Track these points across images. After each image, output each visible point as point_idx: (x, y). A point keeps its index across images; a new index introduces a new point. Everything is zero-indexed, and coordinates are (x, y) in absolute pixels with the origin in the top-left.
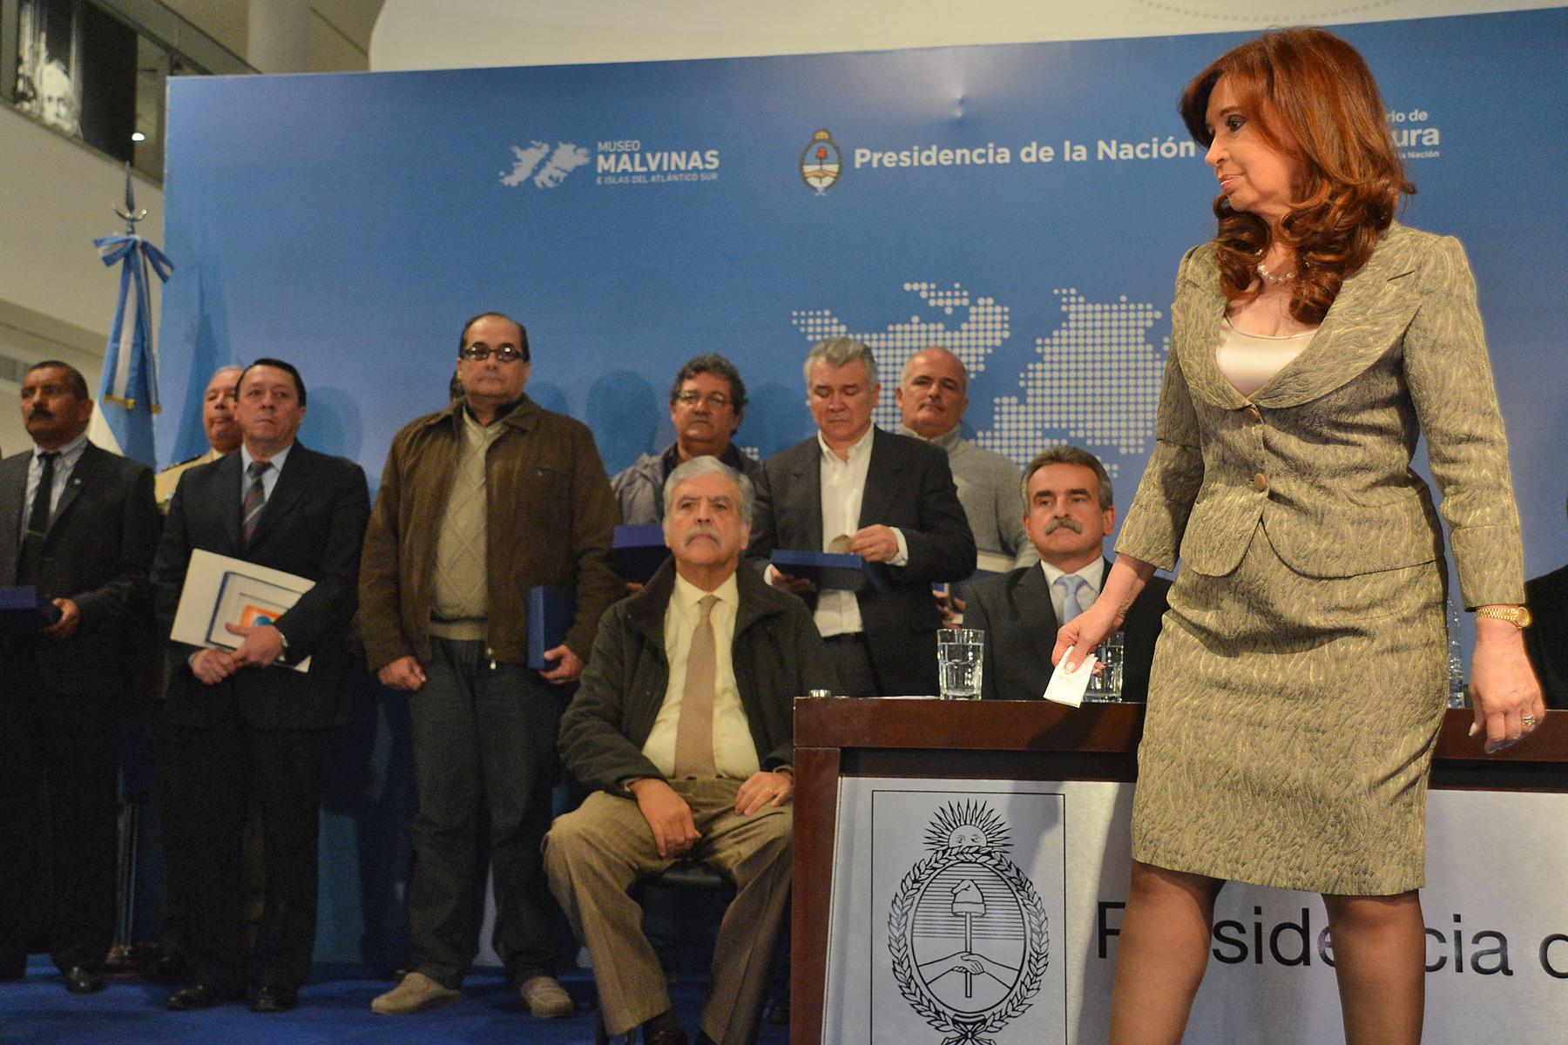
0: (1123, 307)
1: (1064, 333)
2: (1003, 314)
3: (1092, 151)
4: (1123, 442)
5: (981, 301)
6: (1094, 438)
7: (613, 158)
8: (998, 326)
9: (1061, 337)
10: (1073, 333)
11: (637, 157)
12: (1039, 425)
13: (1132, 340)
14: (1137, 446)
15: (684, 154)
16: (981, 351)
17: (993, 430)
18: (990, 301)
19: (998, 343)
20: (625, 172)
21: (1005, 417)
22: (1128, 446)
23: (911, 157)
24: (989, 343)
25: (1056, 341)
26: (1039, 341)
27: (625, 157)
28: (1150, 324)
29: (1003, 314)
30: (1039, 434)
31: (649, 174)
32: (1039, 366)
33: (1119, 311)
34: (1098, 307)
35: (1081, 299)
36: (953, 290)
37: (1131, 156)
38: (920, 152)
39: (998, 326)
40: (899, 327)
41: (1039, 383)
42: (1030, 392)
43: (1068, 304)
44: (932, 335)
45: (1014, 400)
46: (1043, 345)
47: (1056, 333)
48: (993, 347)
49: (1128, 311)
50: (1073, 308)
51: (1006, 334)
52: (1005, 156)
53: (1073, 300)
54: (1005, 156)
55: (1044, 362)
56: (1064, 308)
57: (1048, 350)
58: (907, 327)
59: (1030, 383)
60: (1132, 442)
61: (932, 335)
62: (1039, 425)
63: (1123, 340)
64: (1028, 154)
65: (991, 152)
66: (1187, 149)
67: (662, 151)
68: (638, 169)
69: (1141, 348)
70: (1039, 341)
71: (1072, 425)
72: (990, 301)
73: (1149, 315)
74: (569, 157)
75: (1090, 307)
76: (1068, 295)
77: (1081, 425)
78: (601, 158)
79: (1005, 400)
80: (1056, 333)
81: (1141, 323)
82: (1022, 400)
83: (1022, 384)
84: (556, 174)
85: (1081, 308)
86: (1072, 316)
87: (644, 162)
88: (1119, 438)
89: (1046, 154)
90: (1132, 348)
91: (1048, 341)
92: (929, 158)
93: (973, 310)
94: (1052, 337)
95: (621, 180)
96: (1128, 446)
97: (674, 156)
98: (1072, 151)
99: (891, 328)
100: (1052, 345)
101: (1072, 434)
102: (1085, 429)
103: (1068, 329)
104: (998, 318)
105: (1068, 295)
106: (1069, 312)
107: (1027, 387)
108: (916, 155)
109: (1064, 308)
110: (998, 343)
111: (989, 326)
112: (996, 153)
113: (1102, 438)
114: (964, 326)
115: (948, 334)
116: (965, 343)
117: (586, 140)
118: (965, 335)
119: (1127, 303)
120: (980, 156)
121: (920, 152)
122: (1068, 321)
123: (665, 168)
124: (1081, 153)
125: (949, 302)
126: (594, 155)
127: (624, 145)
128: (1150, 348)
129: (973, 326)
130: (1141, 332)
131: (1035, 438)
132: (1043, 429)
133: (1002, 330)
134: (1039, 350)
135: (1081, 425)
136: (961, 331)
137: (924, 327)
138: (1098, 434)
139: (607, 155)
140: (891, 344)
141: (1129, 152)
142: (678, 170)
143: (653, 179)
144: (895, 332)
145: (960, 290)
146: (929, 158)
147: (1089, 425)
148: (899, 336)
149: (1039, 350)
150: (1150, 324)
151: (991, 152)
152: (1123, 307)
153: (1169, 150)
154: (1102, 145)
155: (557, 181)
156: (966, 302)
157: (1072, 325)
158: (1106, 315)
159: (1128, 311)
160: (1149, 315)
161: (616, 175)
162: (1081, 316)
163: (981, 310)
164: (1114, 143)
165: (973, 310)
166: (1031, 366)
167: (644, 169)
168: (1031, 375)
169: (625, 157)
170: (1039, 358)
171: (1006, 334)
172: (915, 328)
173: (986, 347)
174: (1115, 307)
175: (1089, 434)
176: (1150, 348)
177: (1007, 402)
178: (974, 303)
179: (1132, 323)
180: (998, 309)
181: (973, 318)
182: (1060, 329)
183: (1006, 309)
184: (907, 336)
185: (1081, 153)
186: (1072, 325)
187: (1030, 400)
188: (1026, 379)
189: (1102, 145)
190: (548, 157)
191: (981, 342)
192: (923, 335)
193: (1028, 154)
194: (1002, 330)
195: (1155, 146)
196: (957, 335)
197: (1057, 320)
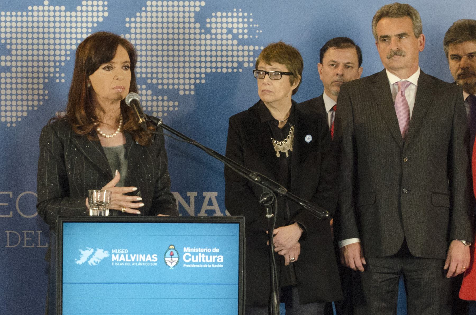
1: (144, 14)
4: (181, 87)
6: (163, 84)
8: (101, 8)
10: (149, 14)
14: (190, 90)
16: (90, 25)
19: (101, 20)
22: (184, 90)
24: (95, 19)
25: (138, 19)
26: (127, 19)
28: (198, 9)
39: (101, 8)
40: (35, 8)
44: (57, 14)
46: (130, 22)
47: (138, 14)
48: (97, 22)
51: (106, 14)
57: (133, 25)
58: (41, 8)
60: (187, 87)
61: (57, 14)
70: (127, 19)
71: (149, 76)
77: (155, 76)
80: (138, 14)
81: (192, 9)
88: (179, 84)
91: (133, 19)
94: (136, 17)
96: (184, 90)
99: (30, 8)
100: (135, 22)
102: (157, 78)
103: (146, 11)
110: (101, 20)
113: (168, 84)
114: (79, 8)
115: (68, 14)
116: (79, 19)
118: (79, 14)
128: (198, 25)
129: (84, 8)
130: (192, 15)
133: (103, 11)
134: (127, 25)
135: (155, 76)
136: (76, 11)
137: (52, 8)
138: (165, 81)
140: (30, 19)
144: (32, 11)
147: (160, 76)
148: (35, 14)
150: (198, 9)
157: (149, 9)
171: (106, 14)
172: (46, 8)
173: (93, 22)
175: (160, 81)
176: (198, 25)
182: (141, 11)
184: (41, 14)
186: (149, 9)
191: (90, 19)
192: (52, 14)
194: (103, 11)
196: (74, 14)
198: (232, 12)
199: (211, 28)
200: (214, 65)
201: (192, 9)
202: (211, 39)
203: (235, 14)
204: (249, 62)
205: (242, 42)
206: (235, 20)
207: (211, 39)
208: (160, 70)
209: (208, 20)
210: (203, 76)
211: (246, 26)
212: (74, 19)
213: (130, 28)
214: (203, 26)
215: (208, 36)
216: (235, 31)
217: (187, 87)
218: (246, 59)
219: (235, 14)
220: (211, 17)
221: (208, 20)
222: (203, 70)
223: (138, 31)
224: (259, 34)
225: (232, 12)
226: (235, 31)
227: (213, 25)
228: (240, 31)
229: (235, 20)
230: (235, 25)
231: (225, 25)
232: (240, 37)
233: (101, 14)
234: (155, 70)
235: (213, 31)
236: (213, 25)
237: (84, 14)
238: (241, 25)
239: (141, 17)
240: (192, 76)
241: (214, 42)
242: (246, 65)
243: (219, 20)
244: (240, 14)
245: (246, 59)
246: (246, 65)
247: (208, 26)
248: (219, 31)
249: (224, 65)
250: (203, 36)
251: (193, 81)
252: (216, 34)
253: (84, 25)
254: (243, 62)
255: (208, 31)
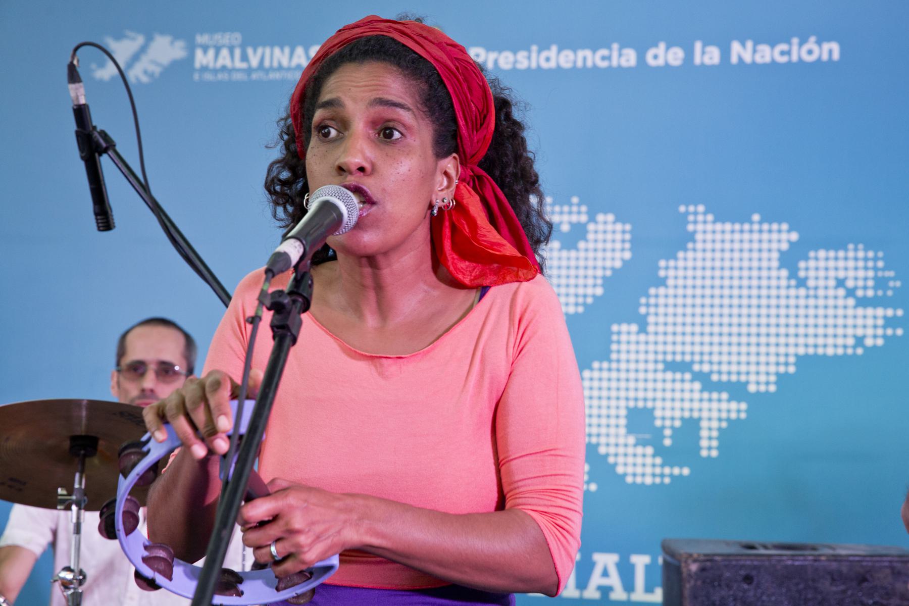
0: (756, 227)
1: (690, 255)
2: (624, 232)
3: (726, 53)
4: (753, 378)
5: (600, 217)
7: (211, 53)
8: (618, 246)
9: (686, 259)
10: (700, 255)
11: (238, 52)
12: (660, 357)
13: (765, 264)
14: (768, 383)
15: (287, 50)
16: (599, 273)
17: (610, 361)
18: (610, 217)
20: (224, 68)
21: (624, 347)
23: (529, 58)
24: (608, 264)
26: (662, 263)
27: (225, 52)
29: (624, 232)
30: (661, 366)
31: (249, 71)
32: (662, 291)
33: (751, 231)
34: (728, 226)
35: (710, 217)
36: (571, 205)
37: (768, 59)
38: (539, 52)
39: (618, 246)
41: (661, 310)
42: (651, 319)
43: (695, 222)
45: (634, 328)
46: (667, 268)
47: (681, 254)
48: (613, 269)
49: (761, 231)
50: (700, 227)
51: (627, 255)
52: (630, 58)
53: (700, 218)
54: (630, 58)
55: (666, 286)
56: (691, 228)
57: (671, 273)
59: (652, 310)
60: (763, 378)
62: (660, 357)
63: (755, 264)
64: (656, 57)
65: (615, 54)
66: (830, 52)
67: (264, 45)
68: (239, 64)
69: (774, 273)
70: (662, 263)
71: (697, 358)
72: (610, 217)
73: (784, 236)
74: (165, 50)
75: (719, 227)
76: (696, 213)
77: (706, 358)
78: (199, 53)
79: (624, 328)
80: (681, 254)
81: (774, 246)
82: (643, 329)
83: (643, 310)
84: (152, 68)
85: (709, 227)
86: (699, 237)
87: (244, 58)
89: (676, 56)
90: (764, 273)
91: (672, 263)
92: (548, 59)
93: (591, 227)
94: (676, 259)
95: (220, 76)
97: (277, 51)
98: (703, 53)
101: (696, 367)
103: (694, 250)
104: (619, 237)
105: (696, 213)
106: (695, 232)
107: (648, 314)
108: (534, 55)
109: (691, 228)
111: (609, 246)
112: (620, 55)
117: (185, 33)
119: (761, 223)
120: (604, 58)
121: (539, 52)
122: (694, 241)
123: (267, 64)
124: (713, 56)
125: (566, 218)
126: (191, 48)
127: (225, 38)
128: (784, 273)
129: (591, 245)
130: (775, 255)
131: (655, 371)
132: (664, 362)
133: (623, 250)
135: (706, 358)
136: (577, 249)
138: (725, 368)
139: (205, 49)
141: (765, 54)
142: (280, 68)
143: (254, 76)
145: (579, 205)
146: (548, 59)
147: (715, 358)
149: (662, 273)
151: (615, 54)
152: (756, 227)
153: (810, 52)
154: (736, 47)
155: (151, 75)
156: (584, 218)
157: (699, 246)
158: (737, 236)
159: (761, 231)
160: (784, 236)
161: (215, 71)
162: (709, 237)
163: (601, 227)
164: (749, 44)
165: (591, 227)
166: (652, 291)
167: (244, 65)
168: (652, 301)
169: (225, 52)
170: (662, 282)
171: (627, 255)
173: (604, 268)
174: (746, 227)
176: (784, 273)
177: (626, 331)
178: (592, 219)
179: (765, 246)
180: (619, 227)
181: (591, 236)
182: (685, 250)
183: (628, 227)
185: (713, 56)
187: (651, 329)
188: (648, 305)
189: (736, 47)
190: (143, 49)
191: (599, 263)
193: (656, 57)
194: (623, 250)
195: (795, 49)
196: (573, 254)
197: (683, 240)
198: (846, 250)
199: (806, 278)
200: (811, 341)
201: (774, 246)
202: (807, 297)
203: (851, 254)
204: (875, 337)
205: (863, 302)
206: (851, 264)
207: (807, 297)
208: (716, 349)
209: (802, 264)
210: (792, 359)
211: (871, 274)
212: (573, 263)
213: (666, 278)
214: (793, 275)
215: (802, 292)
216: (850, 284)
217: (763, 378)
218: (870, 332)
219: (851, 254)
220: (807, 259)
221: (802, 264)
222: (792, 350)
223: (680, 282)
224: (894, 289)
225: (846, 250)
226: (850, 284)
227: (812, 273)
228: (861, 283)
229: (851, 264)
230: (851, 274)
231: (832, 273)
232: (860, 293)
233: (618, 255)
234: (706, 349)
235: (811, 283)
236: (812, 273)
237: (591, 255)
238: (861, 274)
239: (685, 259)
240: (773, 359)
241: (812, 302)
242: (869, 342)
243: (822, 264)
244: (861, 254)
245: (870, 332)
246: (869, 342)
247: (802, 274)
248: (821, 283)
249: (830, 341)
250: (793, 292)
251: (772, 369)
252: (816, 288)
253: (590, 272)
254: (864, 337)
255: (802, 283)
